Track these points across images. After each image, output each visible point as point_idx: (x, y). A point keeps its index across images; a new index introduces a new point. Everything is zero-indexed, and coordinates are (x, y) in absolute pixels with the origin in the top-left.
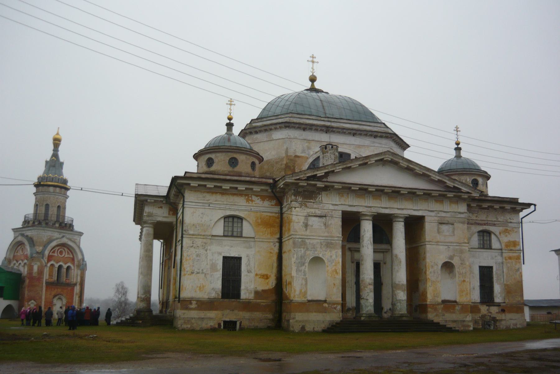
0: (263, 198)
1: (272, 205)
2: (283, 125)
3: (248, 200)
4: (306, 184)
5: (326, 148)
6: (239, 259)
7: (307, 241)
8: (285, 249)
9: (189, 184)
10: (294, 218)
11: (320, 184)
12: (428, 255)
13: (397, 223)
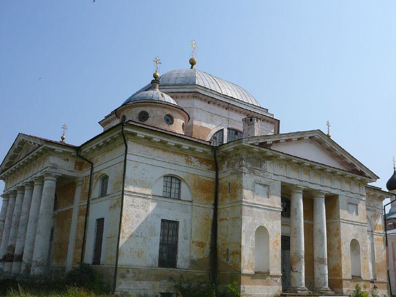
0: (201, 161)
1: (209, 169)
2: (192, 94)
3: (187, 161)
4: (258, 150)
5: (251, 120)
6: (176, 223)
7: (255, 209)
8: (220, 216)
9: (134, 135)
10: (244, 184)
11: (269, 153)
12: (342, 231)
13: (320, 199)
